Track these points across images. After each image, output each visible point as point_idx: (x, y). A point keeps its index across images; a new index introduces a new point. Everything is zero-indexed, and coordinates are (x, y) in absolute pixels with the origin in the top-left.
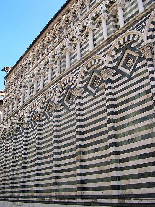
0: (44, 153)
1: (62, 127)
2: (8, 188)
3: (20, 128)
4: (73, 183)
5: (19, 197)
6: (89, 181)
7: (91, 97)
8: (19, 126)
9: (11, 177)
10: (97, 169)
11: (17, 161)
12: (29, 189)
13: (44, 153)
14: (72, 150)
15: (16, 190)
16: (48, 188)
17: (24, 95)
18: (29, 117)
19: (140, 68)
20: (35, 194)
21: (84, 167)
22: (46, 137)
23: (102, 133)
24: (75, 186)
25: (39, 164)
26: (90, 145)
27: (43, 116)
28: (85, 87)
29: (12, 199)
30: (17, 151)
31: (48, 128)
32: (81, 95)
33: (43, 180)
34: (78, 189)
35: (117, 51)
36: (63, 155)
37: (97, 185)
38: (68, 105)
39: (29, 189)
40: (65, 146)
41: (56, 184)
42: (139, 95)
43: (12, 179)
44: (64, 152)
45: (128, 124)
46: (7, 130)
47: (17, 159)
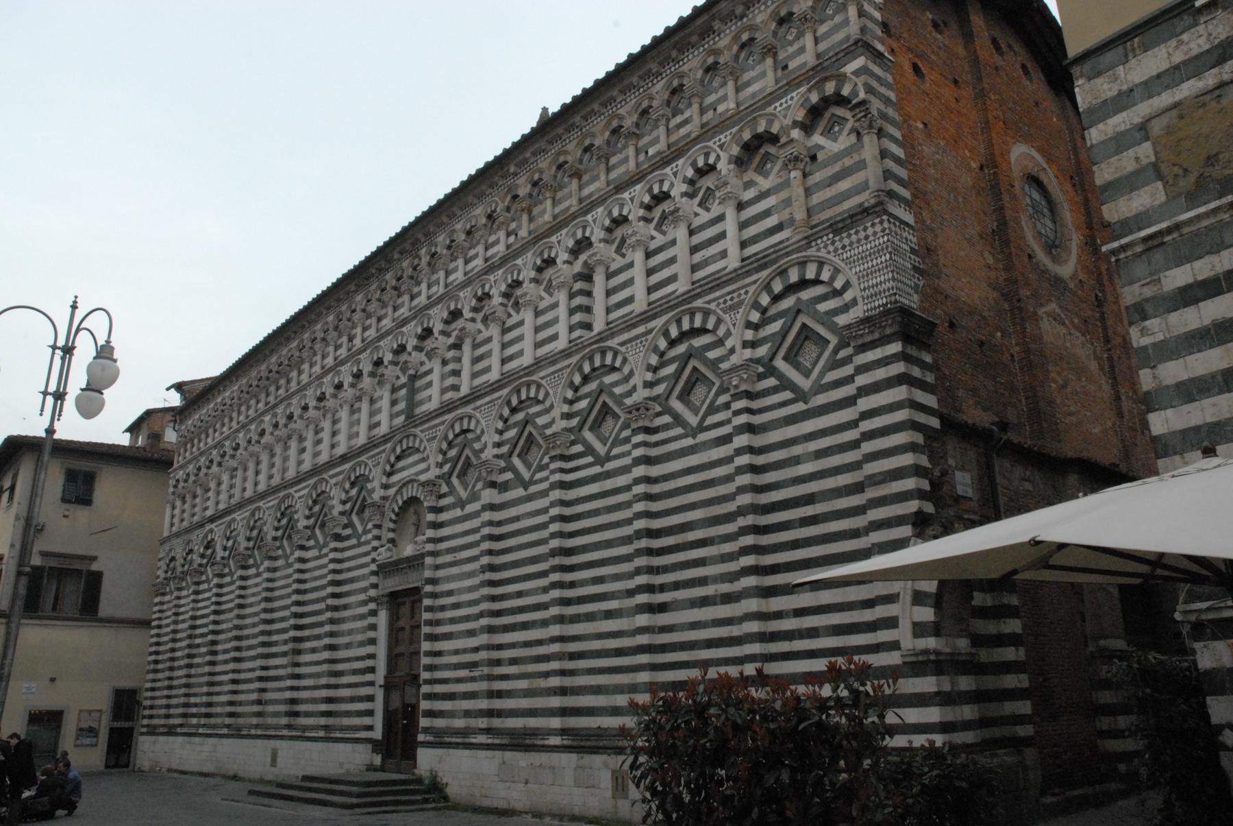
2: (177, 706)
5: (198, 726)
6: (307, 701)
8: (205, 561)
9: (184, 681)
11: (198, 646)
12: (219, 710)
13: (247, 637)
15: (194, 710)
18: (225, 549)
19: (369, 531)
20: (228, 721)
21: (298, 677)
27: (250, 556)
29: (184, 730)
30: (199, 622)
31: (256, 587)
32: (304, 543)
35: (353, 484)
36: (274, 650)
38: (288, 551)
39: (219, 710)
41: (259, 702)
42: (363, 577)
43: (187, 686)
46: (178, 564)
47: (198, 641)
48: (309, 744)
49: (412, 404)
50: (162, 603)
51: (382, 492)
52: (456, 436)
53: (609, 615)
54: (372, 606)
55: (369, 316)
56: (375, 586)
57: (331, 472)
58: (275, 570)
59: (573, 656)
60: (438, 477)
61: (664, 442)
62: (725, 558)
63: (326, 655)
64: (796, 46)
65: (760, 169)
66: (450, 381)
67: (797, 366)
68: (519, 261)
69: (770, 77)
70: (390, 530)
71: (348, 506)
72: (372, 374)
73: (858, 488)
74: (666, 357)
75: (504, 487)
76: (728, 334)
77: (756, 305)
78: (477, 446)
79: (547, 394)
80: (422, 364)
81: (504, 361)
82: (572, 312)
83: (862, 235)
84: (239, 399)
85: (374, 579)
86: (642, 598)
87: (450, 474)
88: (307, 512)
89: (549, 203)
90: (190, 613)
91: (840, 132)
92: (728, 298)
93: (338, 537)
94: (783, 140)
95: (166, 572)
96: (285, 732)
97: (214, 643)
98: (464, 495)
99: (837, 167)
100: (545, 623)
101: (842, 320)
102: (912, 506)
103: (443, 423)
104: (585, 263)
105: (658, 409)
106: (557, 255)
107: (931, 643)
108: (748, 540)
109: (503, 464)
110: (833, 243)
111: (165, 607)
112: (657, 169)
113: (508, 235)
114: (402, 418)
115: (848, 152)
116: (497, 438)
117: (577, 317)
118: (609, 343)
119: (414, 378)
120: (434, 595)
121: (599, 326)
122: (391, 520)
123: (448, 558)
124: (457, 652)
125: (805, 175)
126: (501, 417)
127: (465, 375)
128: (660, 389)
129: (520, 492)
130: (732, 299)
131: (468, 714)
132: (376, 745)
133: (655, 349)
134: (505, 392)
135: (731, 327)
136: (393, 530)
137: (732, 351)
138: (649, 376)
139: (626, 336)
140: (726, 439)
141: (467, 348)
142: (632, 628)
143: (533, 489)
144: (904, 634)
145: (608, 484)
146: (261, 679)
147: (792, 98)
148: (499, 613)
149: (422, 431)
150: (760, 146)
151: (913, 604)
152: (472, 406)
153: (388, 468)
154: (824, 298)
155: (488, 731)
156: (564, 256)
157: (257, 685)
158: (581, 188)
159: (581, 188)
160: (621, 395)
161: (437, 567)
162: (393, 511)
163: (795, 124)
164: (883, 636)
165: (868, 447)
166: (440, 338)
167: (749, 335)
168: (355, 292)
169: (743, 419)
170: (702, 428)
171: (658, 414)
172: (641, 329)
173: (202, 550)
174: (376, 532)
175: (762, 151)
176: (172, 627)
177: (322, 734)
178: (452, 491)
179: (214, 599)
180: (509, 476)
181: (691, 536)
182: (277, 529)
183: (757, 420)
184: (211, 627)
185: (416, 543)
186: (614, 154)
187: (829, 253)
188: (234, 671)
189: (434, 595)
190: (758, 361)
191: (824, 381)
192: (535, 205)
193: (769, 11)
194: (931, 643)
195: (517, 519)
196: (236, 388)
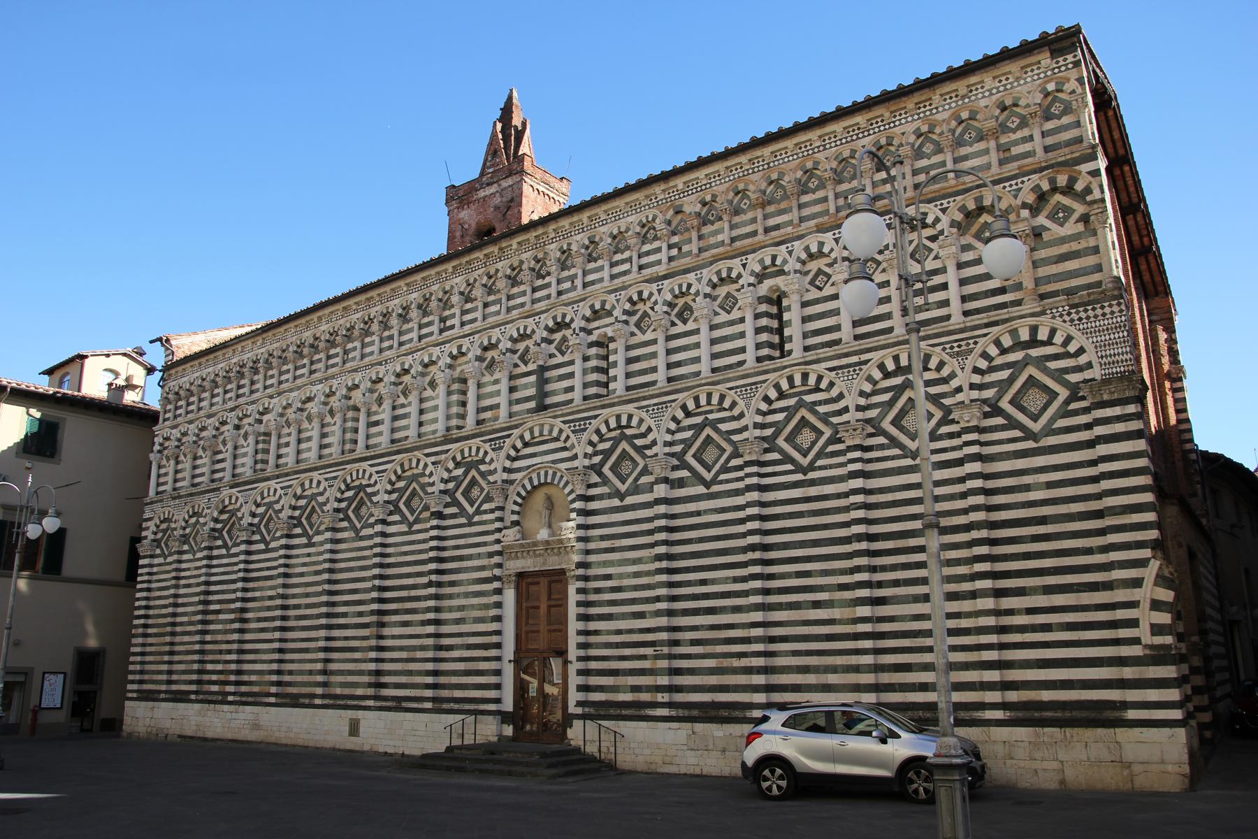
0: (297, 607)
1: (343, 565)
3: (224, 533)
4: (360, 673)
6: (390, 673)
7: (404, 528)
8: (219, 526)
10: (404, 655)
13: (297, 607)
14: (360, 614)
16: (306, 678)
17: (236, 448)
18: (254, 515)
19: (485, 512)
20: (273, 690)
22: (302, 575)
23: (418, 599)
24: (366, 679)
25: (283, 629)
26: (396, 612)
27: (295, 526)
28: (395, 504)
30: (213, 588)
33: (292, 661)
34: (370, 685)
35: (458, 465)
36: (341, 621)
37: (403, 679)
40: (347, 603)
42: (479, 556)
44: (345, 615)
45: (458, 595)
47: (212, 607)
48: (409, 715)
49: (542, 394)
50: (151, 566)
51: (505, 476)
52: (610, 430)
53: (817, 605)
54: (496, 585)
55: (468, 299)
56: (500, 566)
57: (426, 451)
58: (338, 541)
59: (772, 640)
63: (430, 629)
64: (1019, 135)
66: (594, 377)
67: (1022, 409)
68: (691, 277)
69: (994, 157)
70: (513, 512)
71: (451, 485)
72: (480, 359)
73: (1099, 514)
74: (878, 387)
75: (681, 483)
76: (953, 375)
77: (985, 355)
78: (639, 442)
79: (734, 404)
80: (551, 356)
81: (670, 366)
82: (758, 331)
83: (1099, 312)
84: (267, 361)
85: (497, 559)
86: (864, 593)
88: (389, 487)
89: (726, 226)
90: (203, 579)
91: (1066, 219)
93: (439, 515)
94: (1012, 217)
95: (155, 533)
96: (371, 703)
97: (243, 610)
98: (623, 488)
99: (1064, 249)
100: (737, 609)
101: (1074, 378)
102: (1153, 534)
103: (596, 417)
105: (870, 430)
106: (739, 276)
107: (1168, 640)
108: (984, 550)
109: (676, 462)
110: (1069, 314)
111: (155, 570)
113: (670, 247)
114: (532, 404)
115: (1076, 237)
116: (669, 438)
117: (764, 337)
119: (543, 369)
120: (586, 578)
121: (795, 346)
122: (515, 503)
123: (605, 544)
124: (619, 632)
125: (1032, 250)
126: (674, 419)
127: (618, 372)
128: (873, 413)
129: (701, 490)
130: (959, 346)
131: (636, 689)
132: (505, 717)
133: (869, 379)
134: (680, 396)
135: (959, 372)
136: (518, 513)
137: (959, 390)
138: (862, 401)
140: (959, 462)
141: (619, 345)
142: (846, 616)
143: (715, 488)
144: (1143, 632)
145: (813, 491)
146: (326, 650)
147: (1023, 182)
148: (674, 599)
149: (564, 422)
150: (979, 215)
151: (1152, 609)
152: (636, 405)
153: (513, 453)
154: (1056, 357)
155: (670, 705)
156: (747, 279)
157: (321, 655)
158: (766, 217)
159: (766, 217)
161: (588, 552)
162: (519, 494)
163: (1024, 205)
164: (1123, 633)
165: (1106, 485)
166: (582, 334)
167: (977, 379)
168: (453, 273)
169: (974, 449)
171: (871, 435)
172: (854, 359)
173: (215, 514)
174: (498, 514)
175: (982, 220)
176: (172, 591)
177: (429, 705)
178: (606, 481)
179: (242, 566)
180: (684, 473)
182: (340, 501)
184: (239, 594)
185: (550, 526)
186: (807, 193)
187: (1064, 321)
188: (281, 640)
189: (586, 578)
190: (985, 401)
192: (705, 224)
193: (994, 98)
194: (1168, 640)
195: (698, 513)
196: (263, 350)
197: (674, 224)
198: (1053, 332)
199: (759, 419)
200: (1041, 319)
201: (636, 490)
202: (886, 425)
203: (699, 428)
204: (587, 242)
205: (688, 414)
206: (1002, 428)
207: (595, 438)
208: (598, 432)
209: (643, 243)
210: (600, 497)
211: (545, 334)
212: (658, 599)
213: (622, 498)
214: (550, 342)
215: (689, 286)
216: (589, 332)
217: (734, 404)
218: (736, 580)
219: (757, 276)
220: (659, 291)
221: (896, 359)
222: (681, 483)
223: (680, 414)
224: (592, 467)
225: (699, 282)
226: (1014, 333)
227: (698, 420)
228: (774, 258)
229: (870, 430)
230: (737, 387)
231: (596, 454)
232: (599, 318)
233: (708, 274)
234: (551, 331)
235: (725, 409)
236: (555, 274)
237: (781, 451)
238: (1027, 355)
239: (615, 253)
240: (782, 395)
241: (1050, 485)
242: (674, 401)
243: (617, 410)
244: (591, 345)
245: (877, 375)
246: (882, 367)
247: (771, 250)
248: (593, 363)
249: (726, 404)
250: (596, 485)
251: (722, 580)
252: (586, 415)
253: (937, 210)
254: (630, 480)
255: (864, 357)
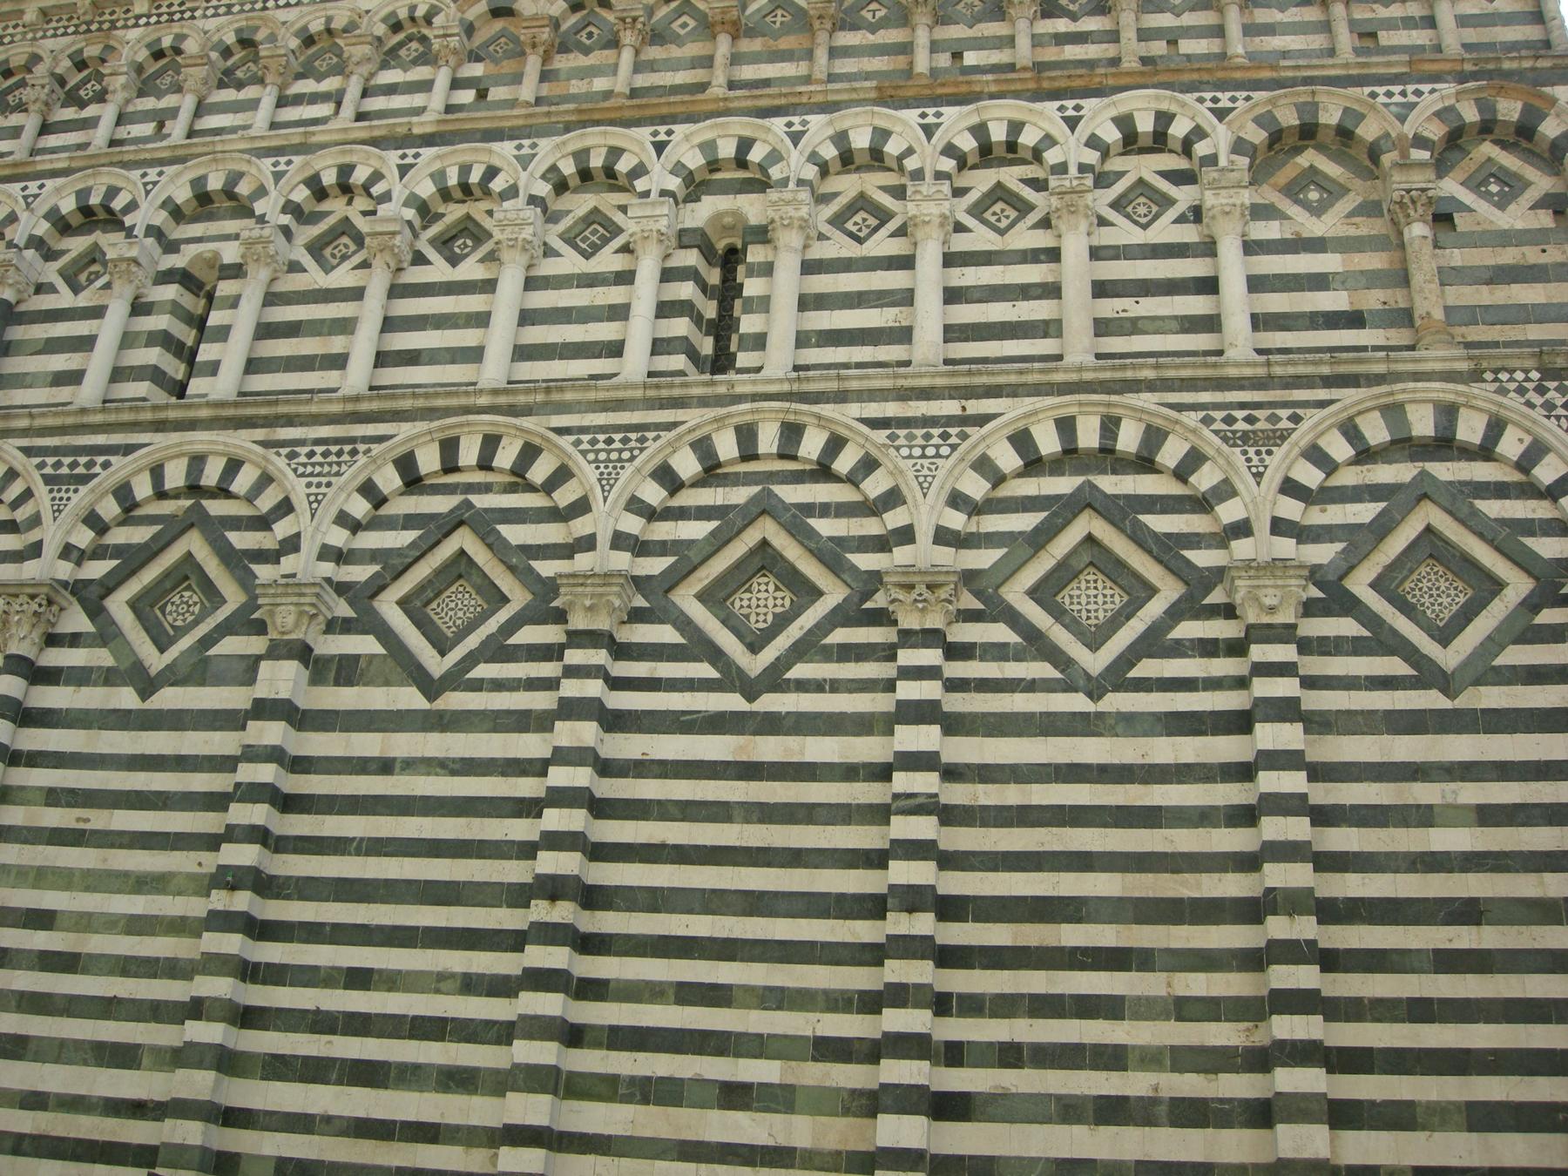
52: (161, 495)
53: (735, 1096)
60: (65, 584)
61: (984, 685)
62: (1183, 1009)
65: (1293, 191)
68: (506, 149)
75: (347, 671)
78: (241, 540)
79: (562, 475)
82: (665, 310)
87: (109, 585)
92: (1240, 414)
100: (458, 1080)
103: (128, 450)
104: (717, 217)
105: (969, 602)
106: (639, 171)
109: (343, 609)
112: (1017, 95)
113: (456, 84)
116: (338, 537)
117: (680, 327)
118: (827, 410)
128: (983, 559)
129: (410, 698)
133: (983, 465)
134: (405, 430)
139: (891, 409)
143: (455, 700)
145: (770, 748)
148: (248, 1017)
150: (1298, 150)
152: (260, 434)
154: (1500, 491)
156: (661, 177)
158: (736, 59)
159: (736, 59)
160: (838, 541)
170: (1117, 677)
172: (950, 407)
178: (107, 634)
180: (367, 645)
181: (1072, 935)
183: (1317, 701)
186: (854, 27)
191: (1498, 662)
192: (564, 49)
195: (385, 766)
197: (480, 38)
198: (1496, 428)
199: (633, 524)
200: (1475, 389)
201: (198, 670)
202: (1016, 593)
203: (438, 528)
204: (230, 39)
205: (413, 482)
206: (1356, 647)
207: (109, 509)
208: (123, 493)
209: (385, 66)
210: (81, 677)
211: (43, 228)
212: (196, 1009)
213: (147, 685)
214: (50, 255)
215: (492, 172)
216: (171, 247)
217: (562, 475)
218: (471, 985)
219: (689, 178)
220: (404, 170)
221: (1066, 426)
222: (347, 671)
223: (389, 480)
224: (78, 589)
225: (524, 166)
226: (1394, 412)
227: (440, 504)
228: (745, 145)
229: (969, 602)
230: (583, 430)
231: (98, 553)
232: (211, 217)
233: (553, 152)
234: (63, 226)
235: (531, 488)
236: (120, 97)
237: (684, 623)
238: (1423, 474)
239: (300, 76)
240: (712, 473)
241: (1487, 815)
242: (380, 439)
243: (200, 440)
244: (165, 277)
245: (1008, 459)
246: (1022, 441)
247: (741, 126)
248: (159, 322)
249: (539, 472)
250: (74, 640)
251: (423, 980)
252: (100, 439)
253: (1203, 109)
254: (185, 643)
255: (976, 407)
